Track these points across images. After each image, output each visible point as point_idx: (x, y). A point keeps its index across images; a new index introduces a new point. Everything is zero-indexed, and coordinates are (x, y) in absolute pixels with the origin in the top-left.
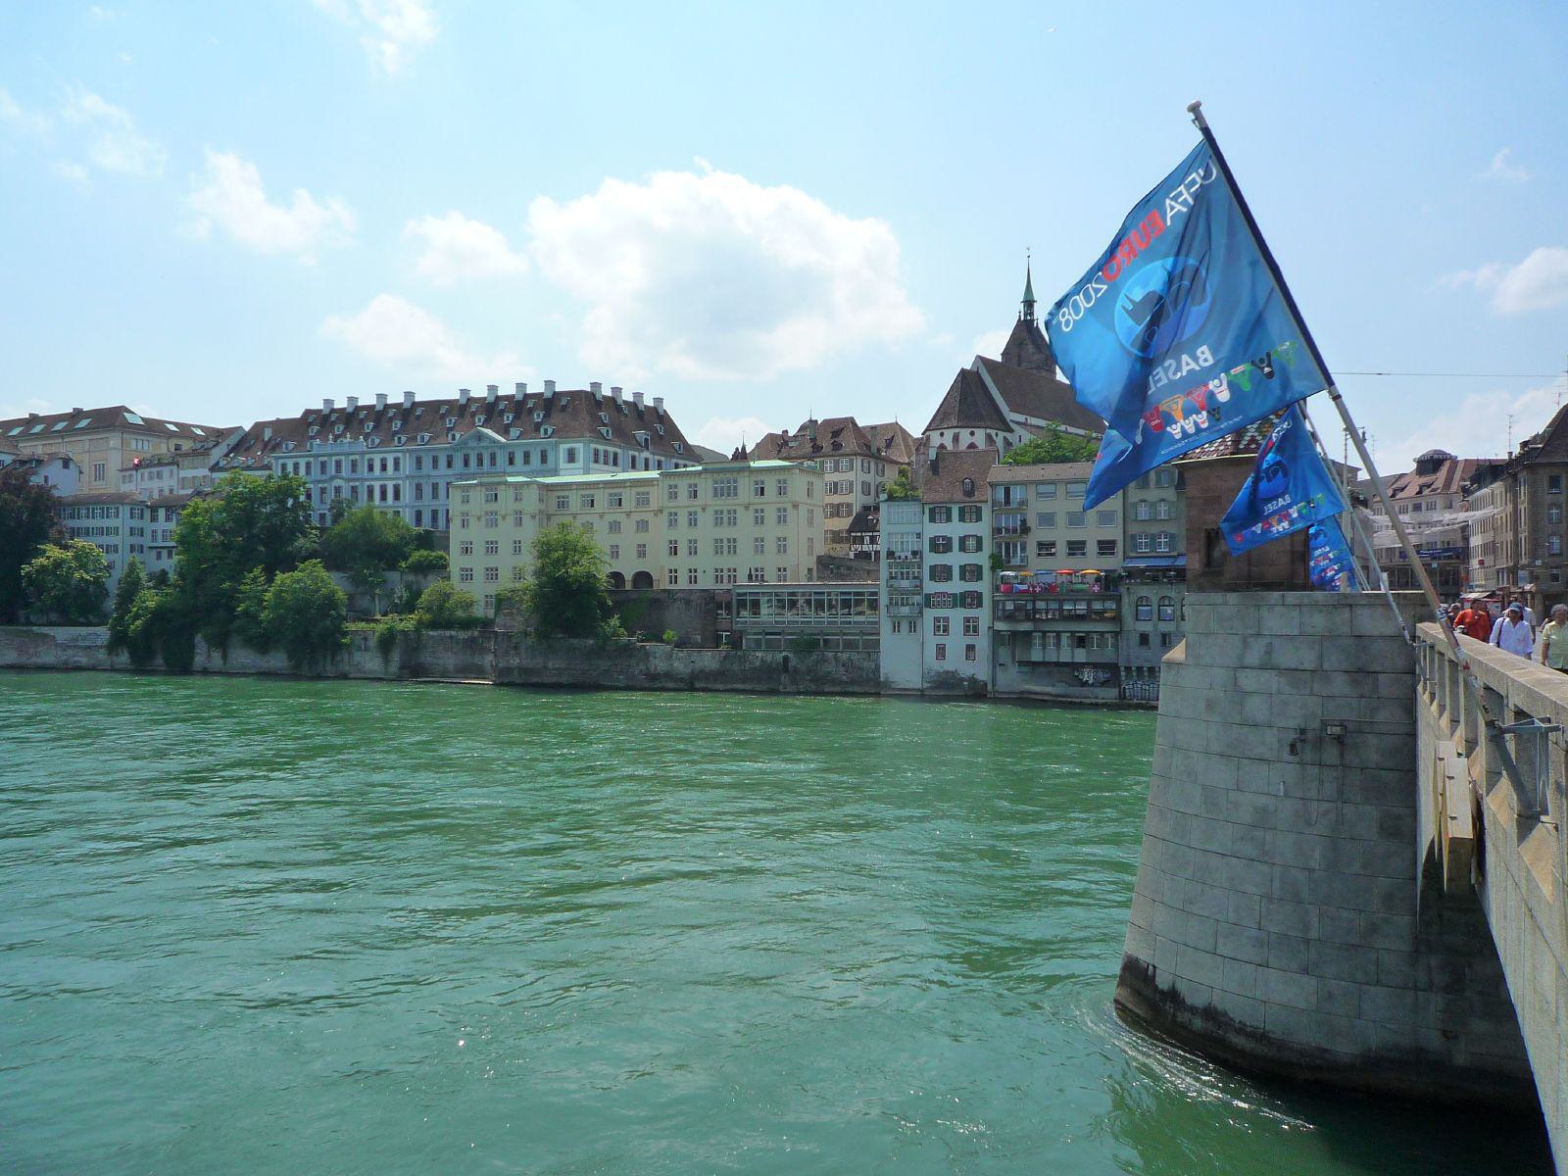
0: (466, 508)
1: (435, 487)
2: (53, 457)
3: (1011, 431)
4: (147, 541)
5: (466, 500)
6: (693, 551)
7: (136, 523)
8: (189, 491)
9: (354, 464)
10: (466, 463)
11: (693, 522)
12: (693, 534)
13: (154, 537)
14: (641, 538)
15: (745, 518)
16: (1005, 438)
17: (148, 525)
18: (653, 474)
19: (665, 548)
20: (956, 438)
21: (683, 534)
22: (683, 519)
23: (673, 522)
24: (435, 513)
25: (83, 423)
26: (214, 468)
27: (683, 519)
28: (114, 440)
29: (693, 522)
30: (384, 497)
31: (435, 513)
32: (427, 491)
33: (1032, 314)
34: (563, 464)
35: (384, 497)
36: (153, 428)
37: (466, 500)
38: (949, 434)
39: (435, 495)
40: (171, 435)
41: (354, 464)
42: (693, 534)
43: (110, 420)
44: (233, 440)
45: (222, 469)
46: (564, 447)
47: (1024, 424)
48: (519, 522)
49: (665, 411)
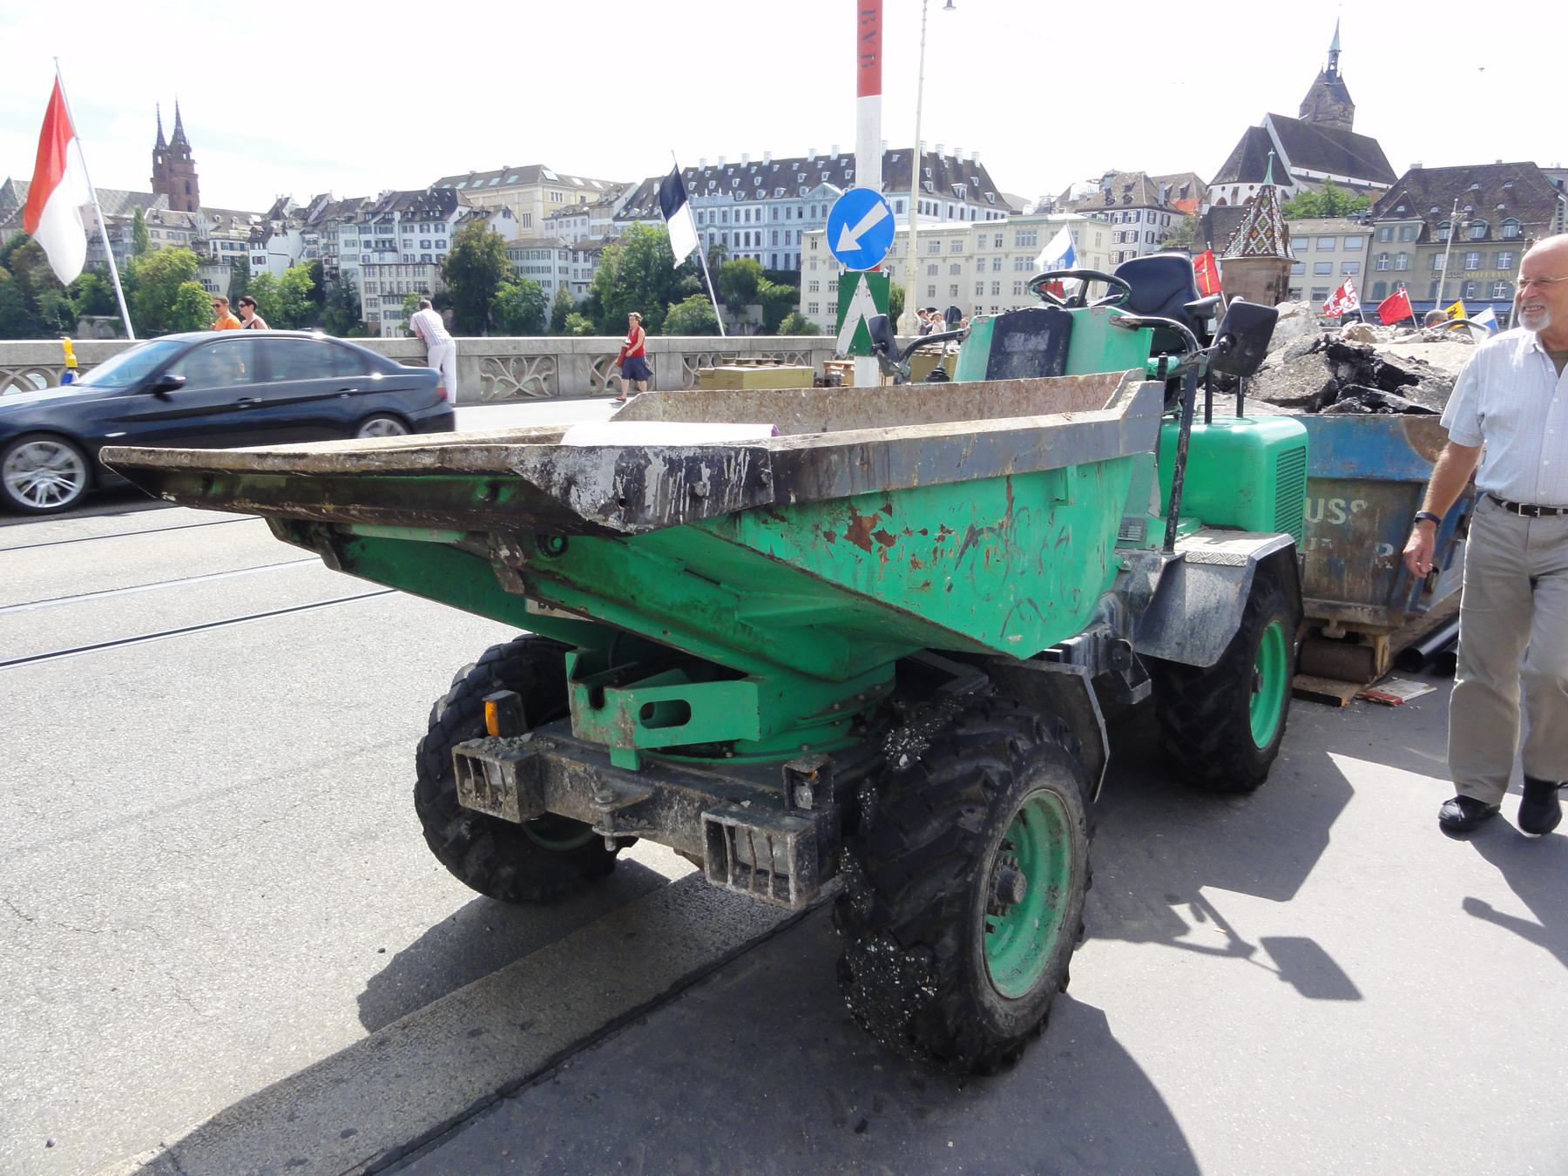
0: (814, 253)
1: (788, 234)
2: (497, 208)
3: (1290, 184)
4: (570, 278)
5: (814, 246)
6: (996, 291)
7: (562, 263)
8: (600, 237)
9: (724, 214)
10: (813, 215)
11: (997, 267)
12: (997, 277)
13: (576, 275)
14: (954, 280)
16: (1283, 192)
17: (572, 266)
18: (967, 224)
19: (973, 290)
20: (1235, 192)
21: (988, 277)
22: (989, 264)
23: (980, 268)
24: (787, 256)
25: (513, 179)
26: (617, 218)
27: (989, 264)
28: (539, 193)
29: (997, 267)
30: (747, 243)
31: (787, 256)
32: (781, 238)
33: (1335, 64)
35: (747, 243)
36: (563, 182)
37: (814, 246)
38: (1230, 188)
39: (788, 242)
40: (578, 188)
41: (724, 214)
42: (997, 277)
43: (530, 175)
44: (629, 194)
45: (623, 219)
47: (1306, 179)
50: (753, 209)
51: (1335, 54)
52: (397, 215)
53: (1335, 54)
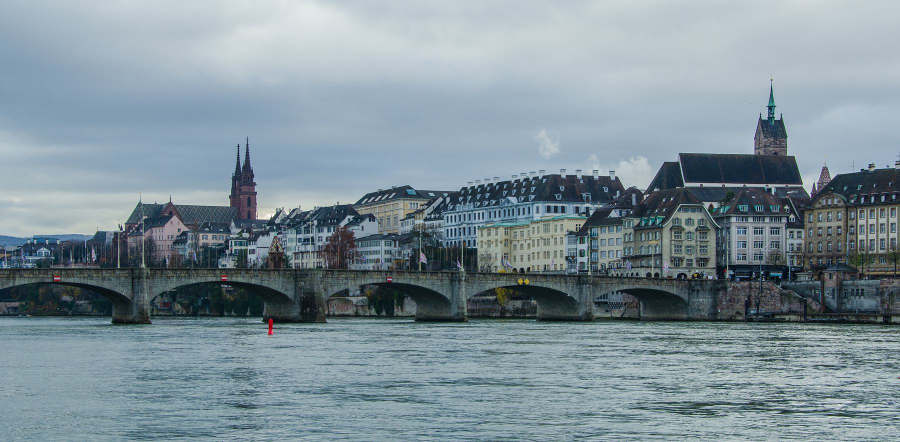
7: (388, 248)
15: (552, 241)
26: (426, 220)
34: (535, 215)
46: (535, 205)
48: (497, 245)
49: (617, 178)
50: (481, 212)
51: (771, 108)
52: (316, 222)
53: (771, 108)
